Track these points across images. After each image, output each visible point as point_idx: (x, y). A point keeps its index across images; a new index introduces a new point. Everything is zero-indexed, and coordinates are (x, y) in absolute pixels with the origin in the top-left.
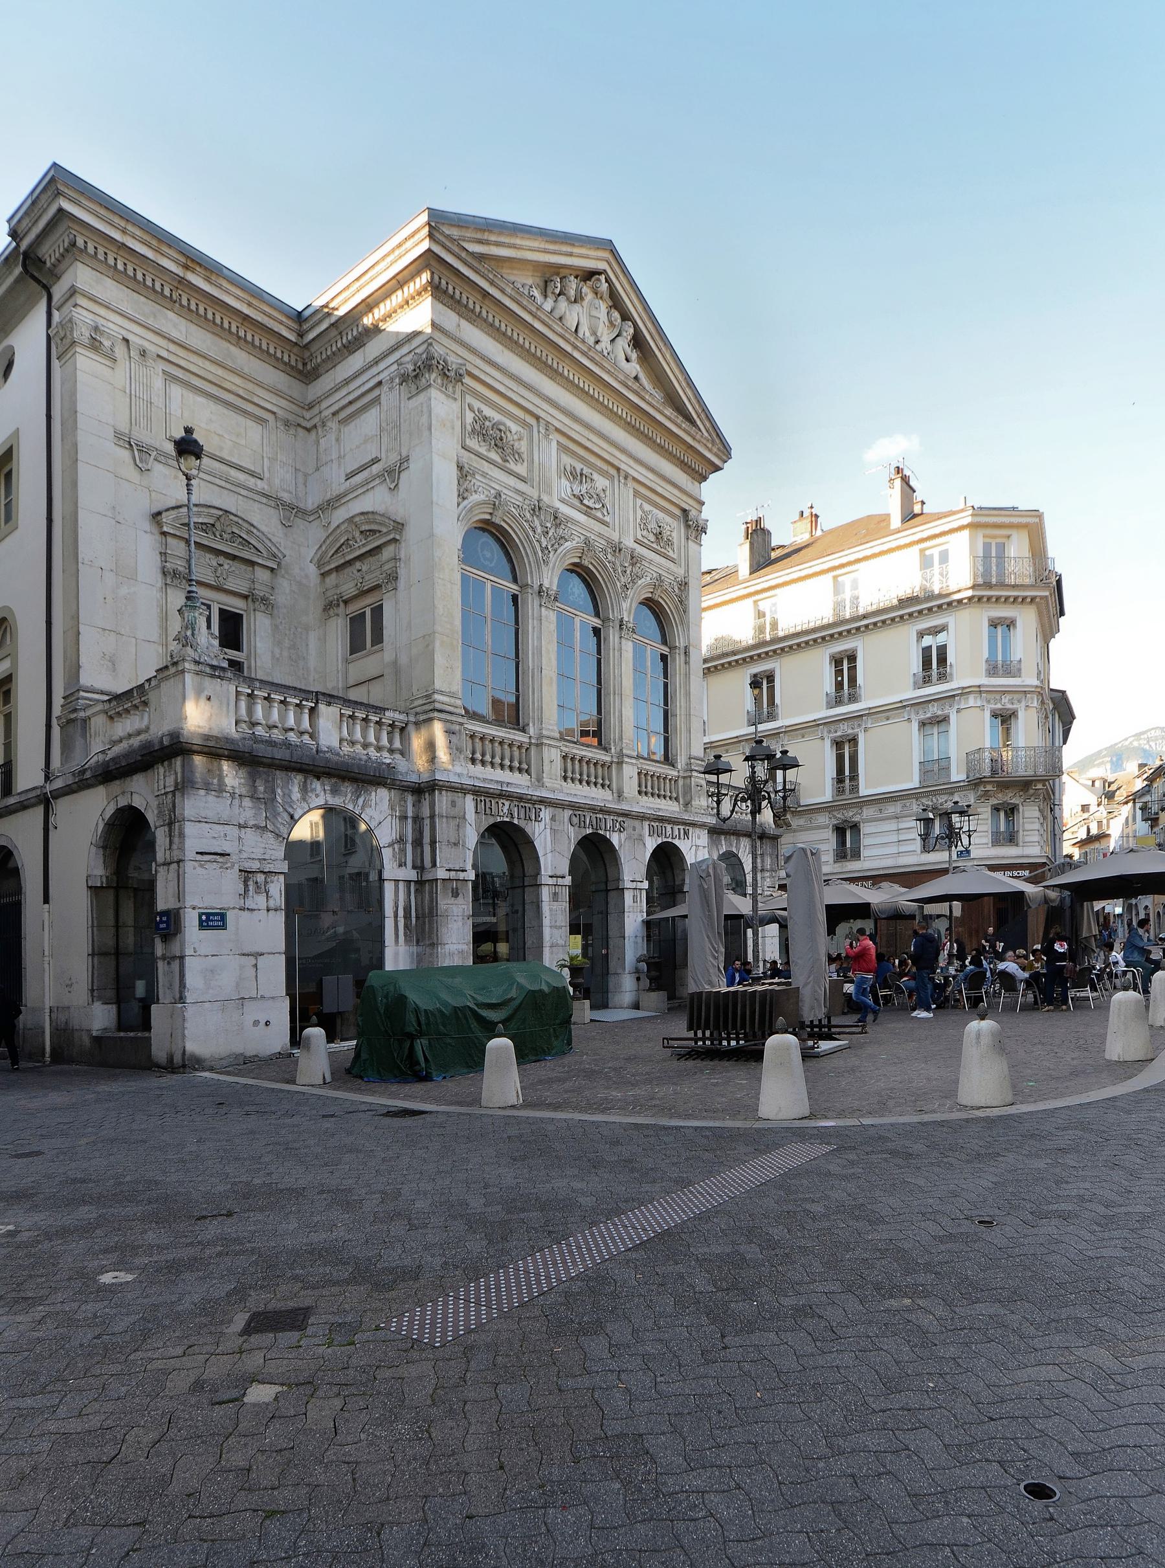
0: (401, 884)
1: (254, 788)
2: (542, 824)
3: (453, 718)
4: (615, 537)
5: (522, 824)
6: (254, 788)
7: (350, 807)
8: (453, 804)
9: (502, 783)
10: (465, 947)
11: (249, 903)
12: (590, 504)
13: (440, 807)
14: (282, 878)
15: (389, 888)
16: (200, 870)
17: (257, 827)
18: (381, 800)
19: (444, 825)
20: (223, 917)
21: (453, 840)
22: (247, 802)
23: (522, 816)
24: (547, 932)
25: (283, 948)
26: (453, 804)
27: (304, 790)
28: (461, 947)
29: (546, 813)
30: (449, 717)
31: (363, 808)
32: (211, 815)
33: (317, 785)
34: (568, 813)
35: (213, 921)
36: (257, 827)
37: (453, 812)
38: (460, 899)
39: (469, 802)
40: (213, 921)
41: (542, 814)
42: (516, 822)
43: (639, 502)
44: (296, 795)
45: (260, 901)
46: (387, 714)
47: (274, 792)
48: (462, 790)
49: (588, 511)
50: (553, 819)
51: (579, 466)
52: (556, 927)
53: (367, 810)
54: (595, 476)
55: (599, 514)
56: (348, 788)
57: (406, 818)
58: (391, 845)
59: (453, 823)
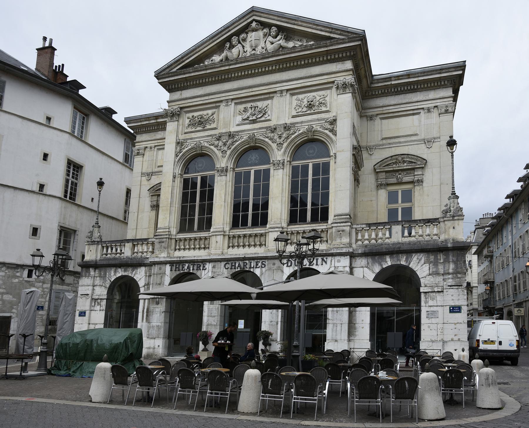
0: (147, 301)
1: (100, 274)
2: (206, 271)
3: (162, 237)
4: (271, 124)
5: (195, 272)
6: (100, 274)
7: (130, 275)
8: (160, 269)
9: (180, 257)
10: (160, 324)
11: (95, 309)
12: (254, 118)
13: (154, 271)
14: (105, 300)
15: (141, 302)
16: (81, 300)
17: (100, 285)
18: (142, 271)
19: (155, 277)
20: (85, 313)
21: (158, 283)
22: (98, 278)
23: (195, 268)
24: (205, 319)
25: (103, 322)
26: (160, 269)
27: (115, 272)
28: (158, 324)
29: (209, 266)
30: (160, 237)
31: (135, 275)
32: (86, 284)
33: (119, 270)
34: (223, 264)
35: (82, 314)
36: (100, 285)
37: (161, 271)
38: (159, 306)
39: (168, 267)
40: (82, 314)
41: (207, 266)
42: (191, 271)
43: (295, 97)
44: (112, 274)
45: (98, 308)
46: (149, 240)
47: (106, 275)
48: (165, 263)
49: (254, 122)
50: (214, 267)
51: (249, 105)
52: (211, 316)
53: (136, 275)
54: (260, 104)
55: (263, 119)
56: (130, 269)
57: (151, 276)
58: (144, 286)
59: (159, 276)
